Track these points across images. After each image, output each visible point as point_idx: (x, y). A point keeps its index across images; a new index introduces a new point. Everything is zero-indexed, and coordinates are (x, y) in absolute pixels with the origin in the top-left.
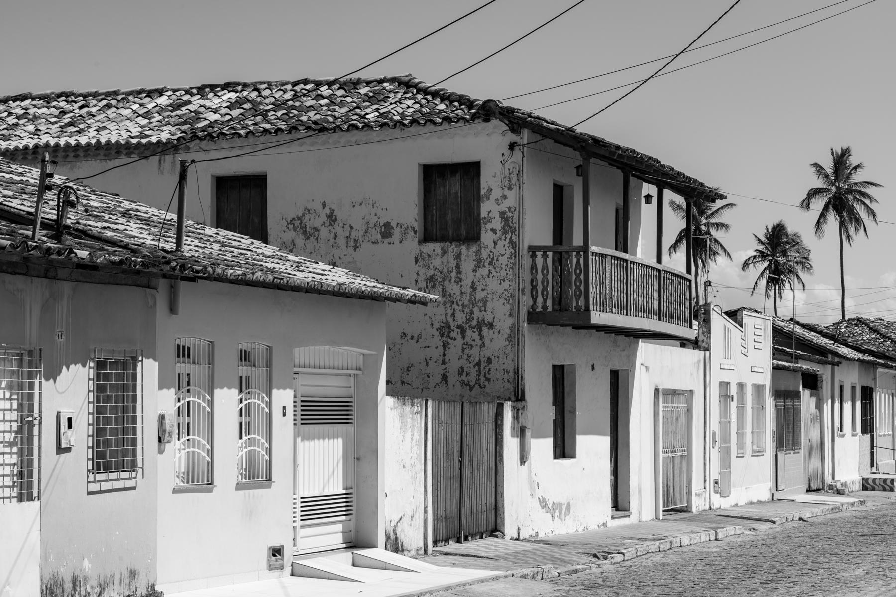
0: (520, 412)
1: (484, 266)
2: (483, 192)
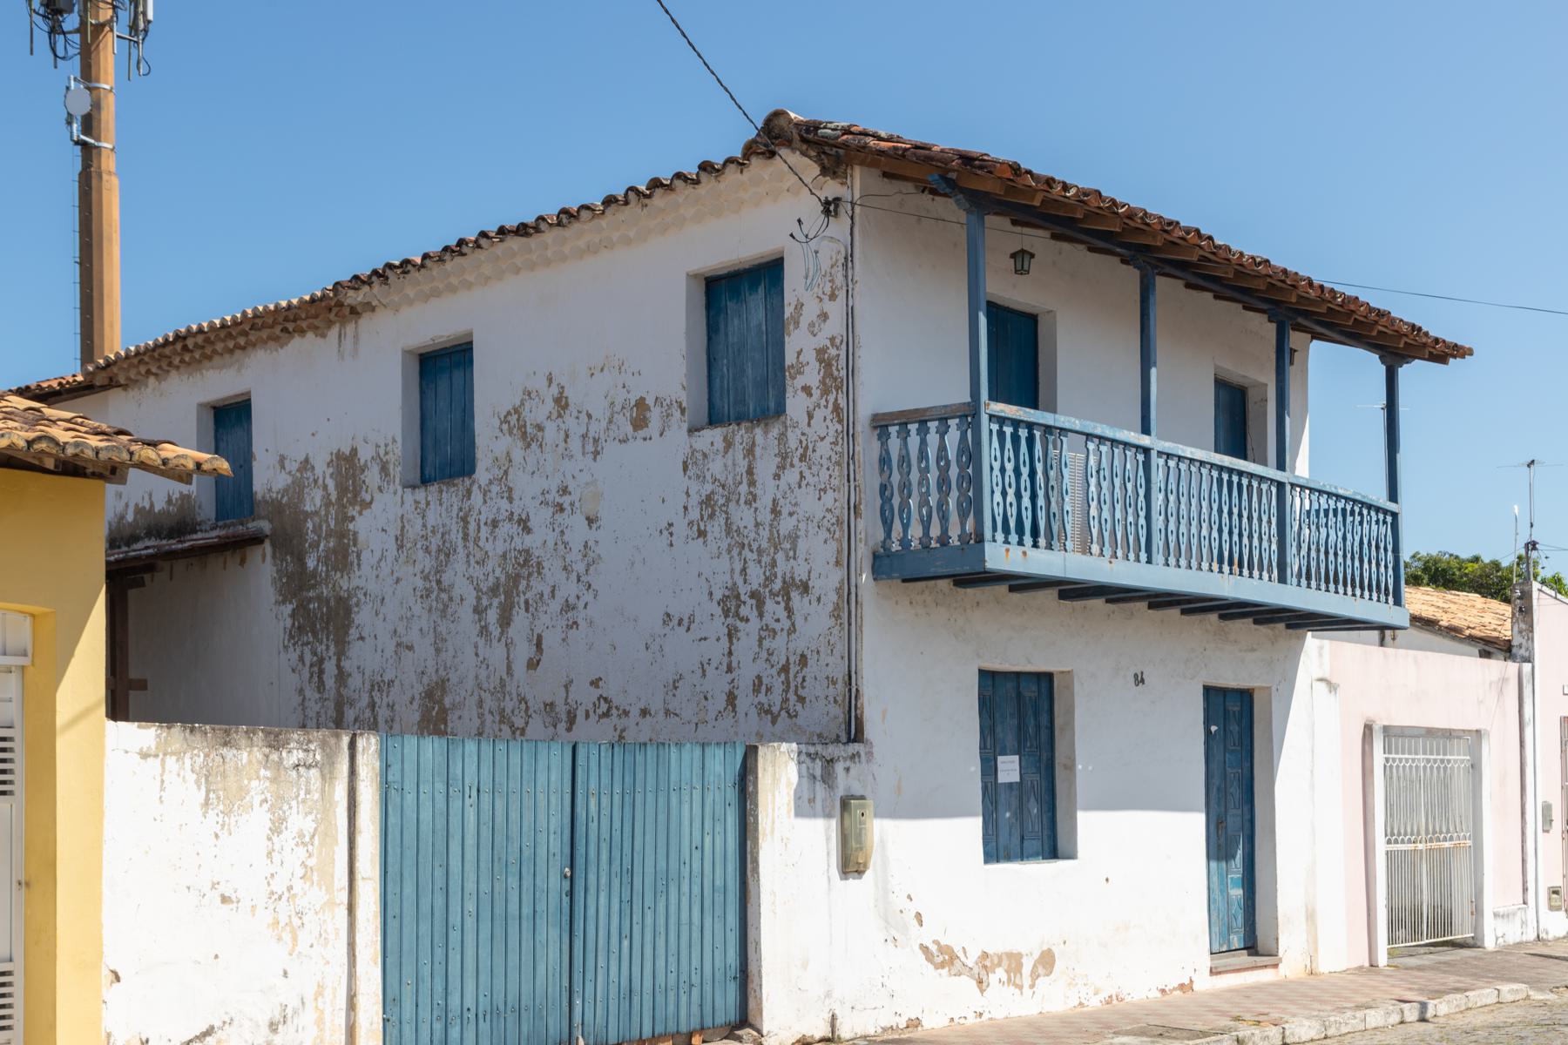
0: (839, 768)
1: (792, 465)
2: (788, 311)
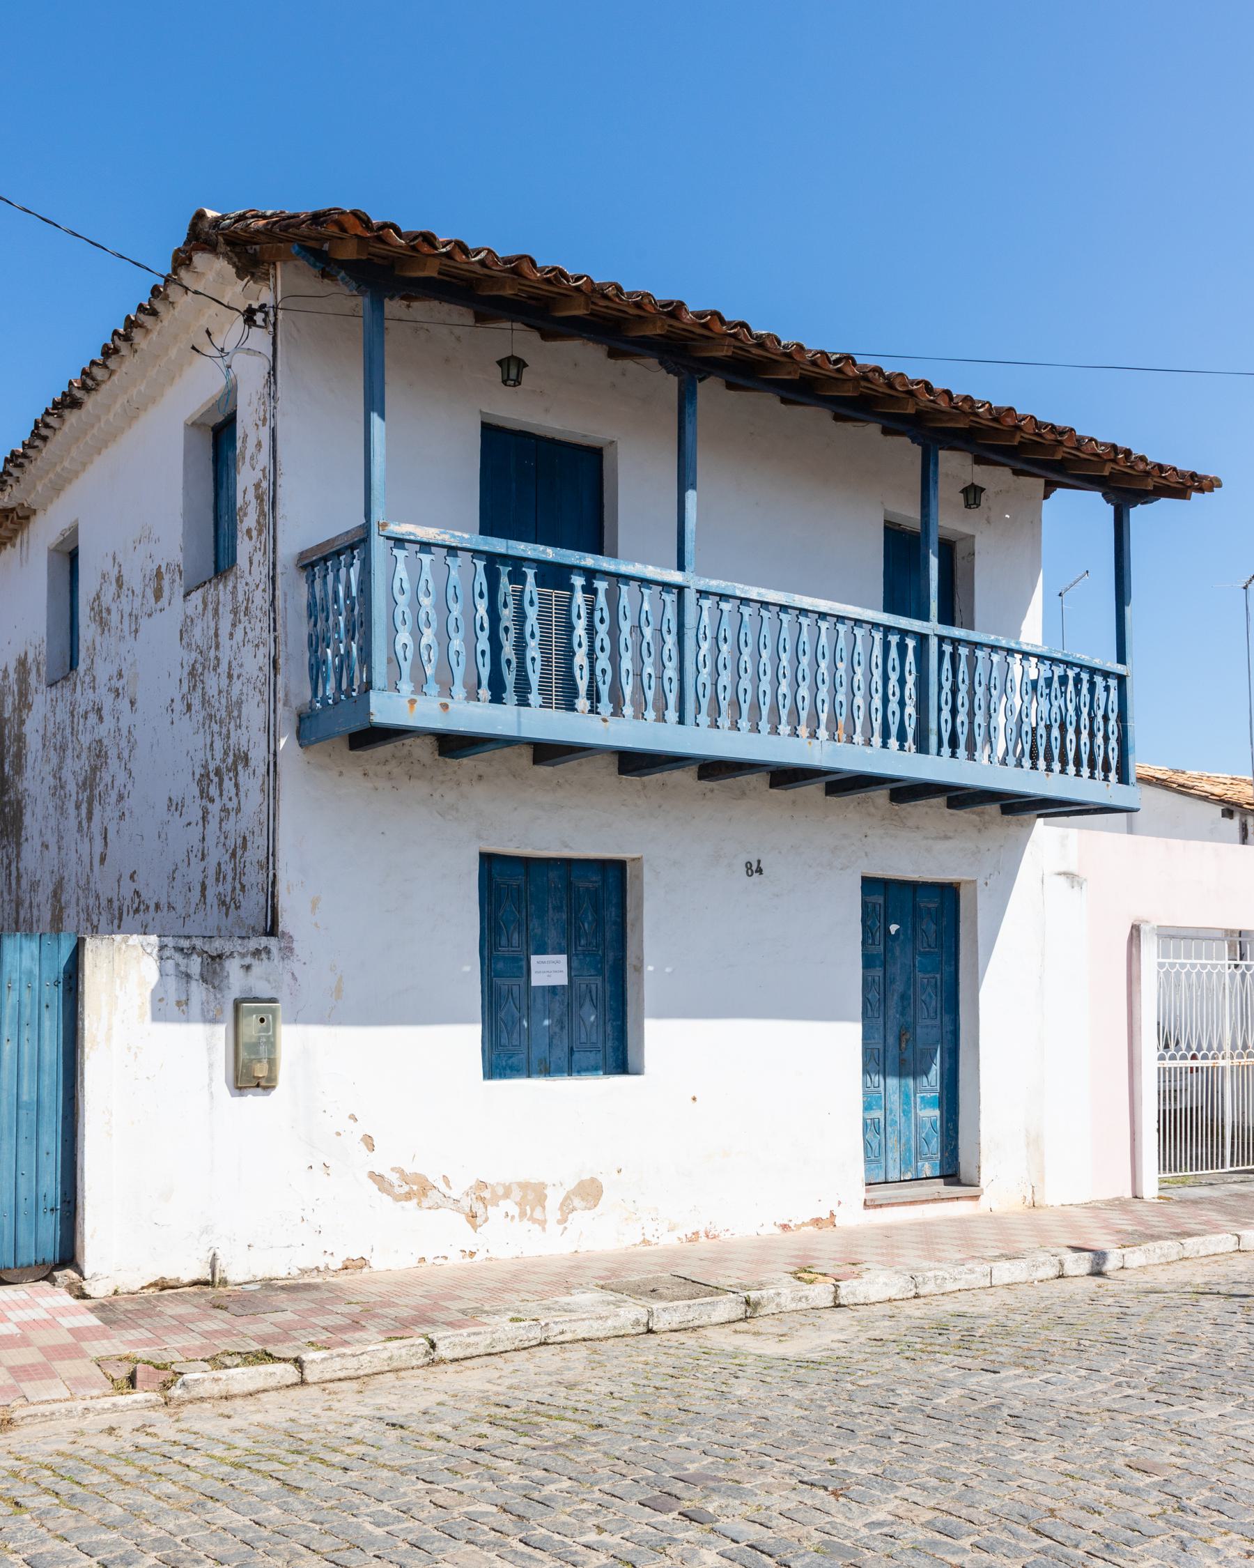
0: (233, 967)
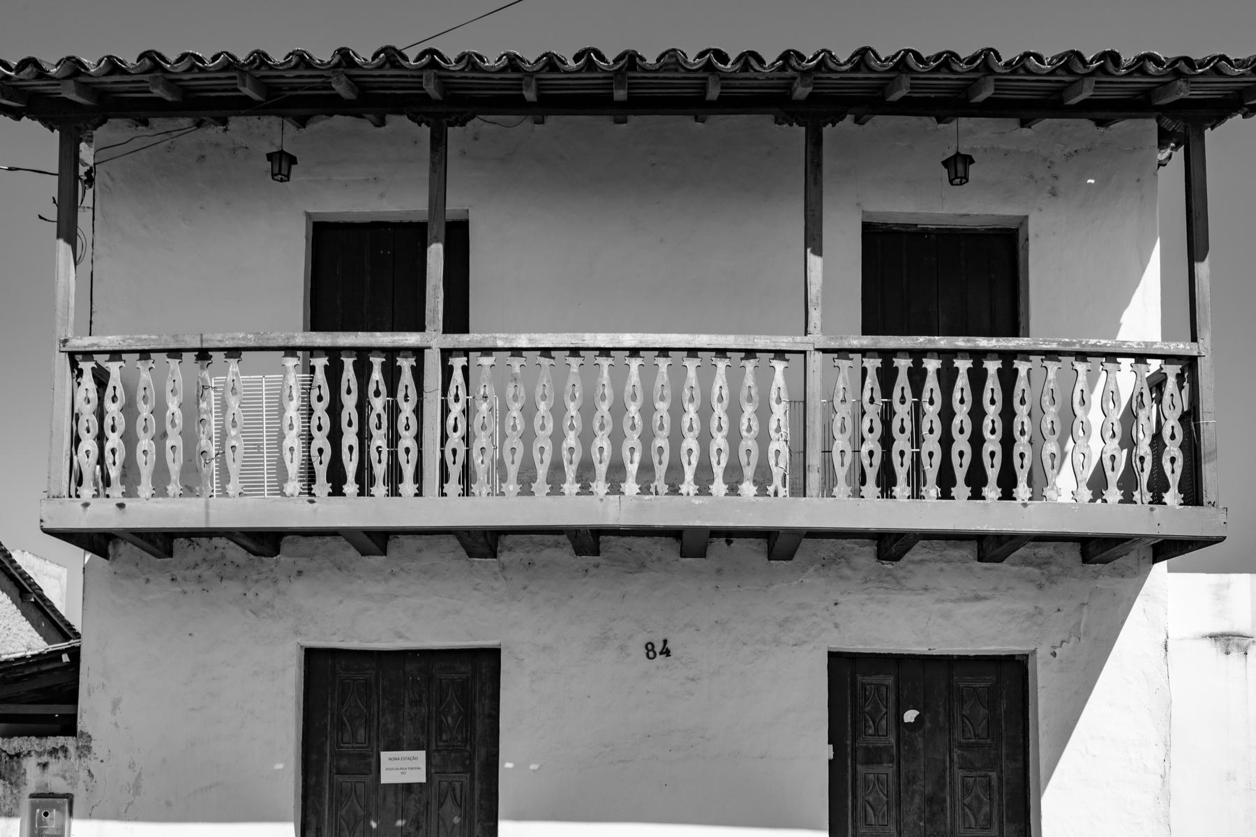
0: (30, 764)
